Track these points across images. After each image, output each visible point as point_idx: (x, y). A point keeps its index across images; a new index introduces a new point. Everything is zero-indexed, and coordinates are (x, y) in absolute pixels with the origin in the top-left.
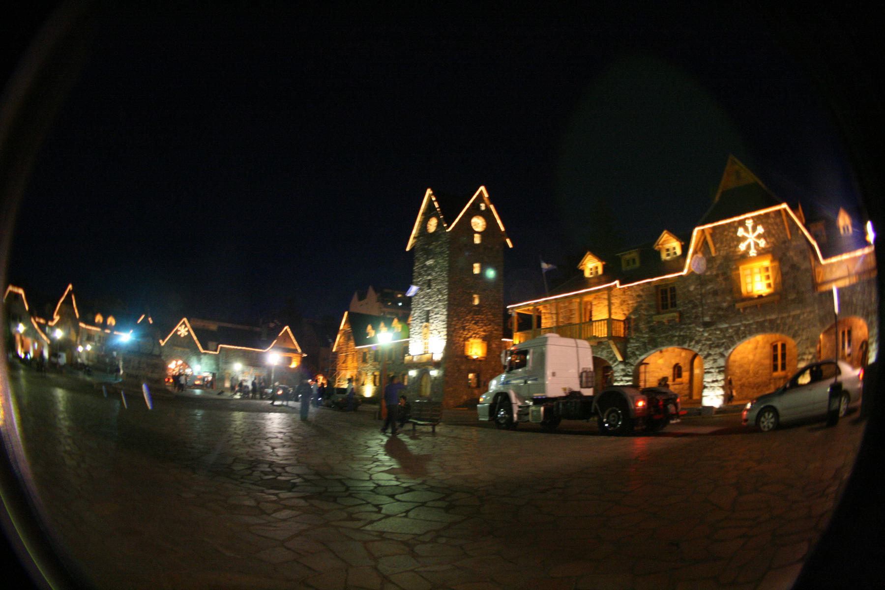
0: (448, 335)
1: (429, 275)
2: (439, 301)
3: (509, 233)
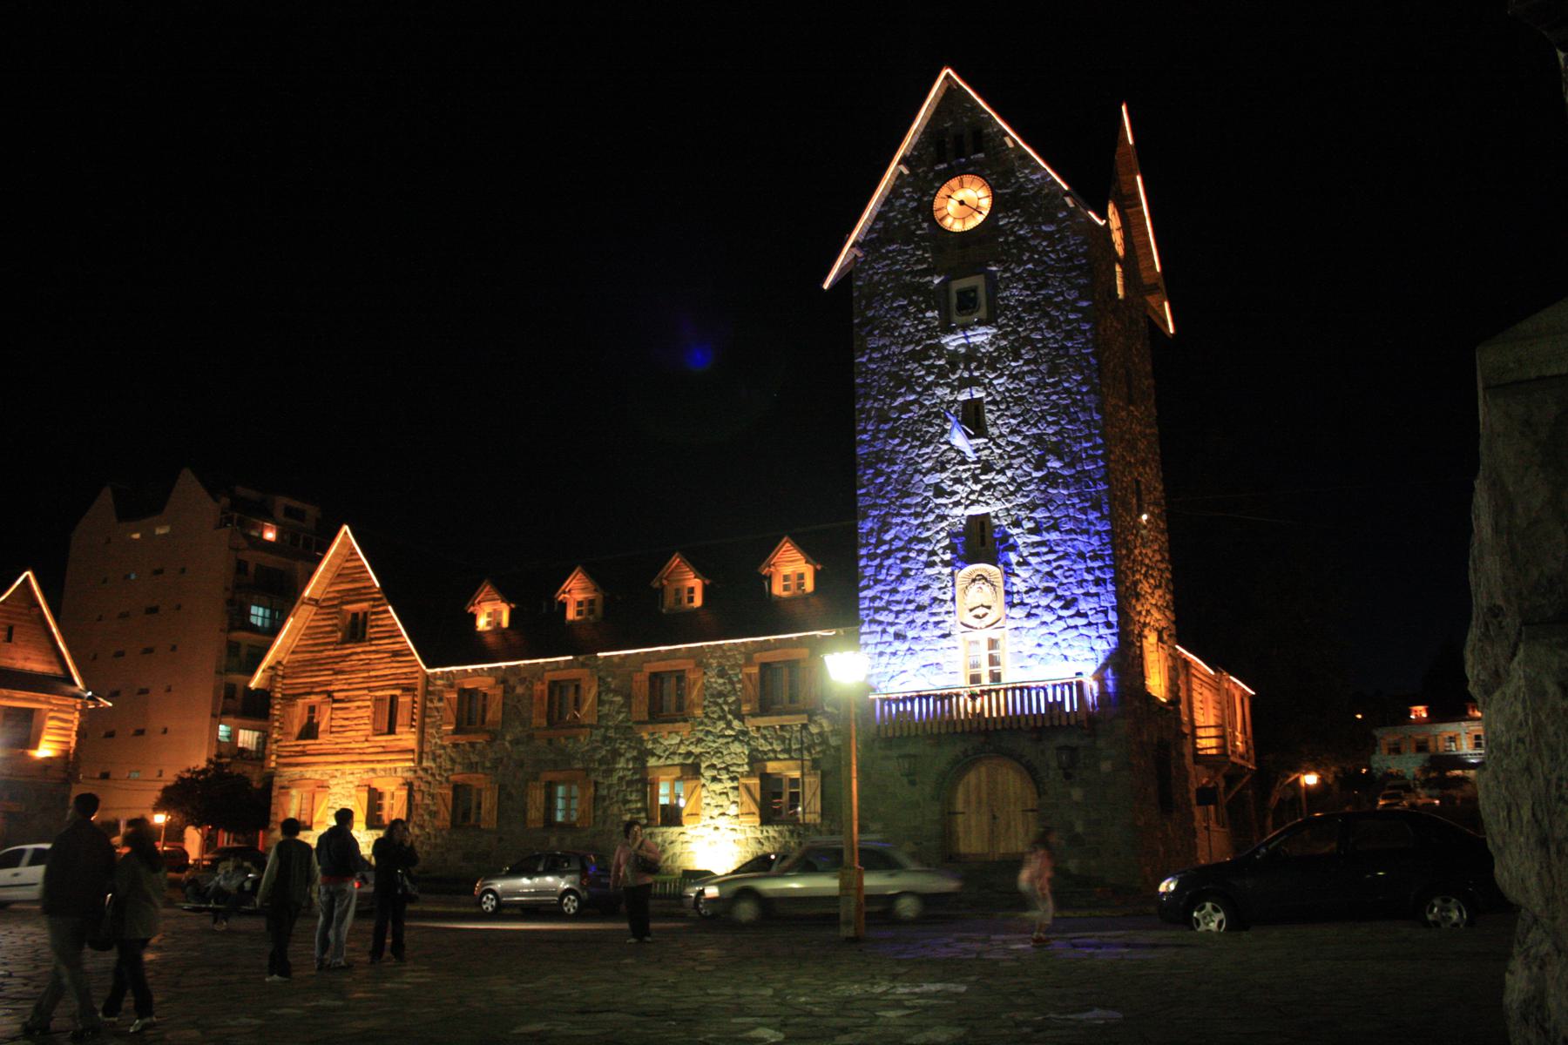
0: (1121, 610)
1: (972, 382)
2: (1051, 479)
3: (1173, 282)
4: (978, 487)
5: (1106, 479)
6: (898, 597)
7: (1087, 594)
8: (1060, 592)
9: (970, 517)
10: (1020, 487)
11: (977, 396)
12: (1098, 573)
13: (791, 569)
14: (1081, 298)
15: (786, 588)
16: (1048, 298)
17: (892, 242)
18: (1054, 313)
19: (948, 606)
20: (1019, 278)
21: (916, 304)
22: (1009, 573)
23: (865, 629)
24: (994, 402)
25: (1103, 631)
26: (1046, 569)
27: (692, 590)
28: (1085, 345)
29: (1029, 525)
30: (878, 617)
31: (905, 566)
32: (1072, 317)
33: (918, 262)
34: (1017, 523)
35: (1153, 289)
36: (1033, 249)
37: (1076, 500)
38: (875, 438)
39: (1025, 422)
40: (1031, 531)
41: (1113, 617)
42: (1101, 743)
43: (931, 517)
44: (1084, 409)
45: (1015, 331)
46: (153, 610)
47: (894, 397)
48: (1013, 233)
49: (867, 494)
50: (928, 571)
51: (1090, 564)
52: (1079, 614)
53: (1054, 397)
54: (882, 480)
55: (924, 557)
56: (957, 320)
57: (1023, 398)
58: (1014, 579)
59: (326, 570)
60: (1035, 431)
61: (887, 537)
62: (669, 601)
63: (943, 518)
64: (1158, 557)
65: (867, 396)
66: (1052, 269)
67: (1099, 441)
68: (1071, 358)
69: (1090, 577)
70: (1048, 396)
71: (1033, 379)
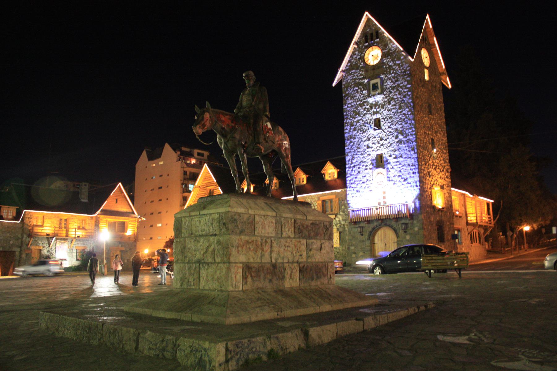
0: (420, 181)
2: (400, 142)
3: (450, 71)
4: (379, 145)
5: (416, 141)
6: (357, 179)
7: (410, 177)
8: (403, 176)
9: (377, 155)
10: (391, 145)
11: (378, 117)
12: (414, 170)
13: (330, 172)
14: (408, 84)
15: (330, 177)
16: (398, 85)
17: (353, 69)
18: (400, 89)
19: (371, 182)
20: (390, 79)
21: (361, 89)
22: (388, 171)
23: (348, 189)
24: (383, 119)
25: (416, 188)
26: (399, 169)
27: (303, 179)
28: (409, 99)
29: (394, 156)
30: (352, 186)
31: (359, 170)
32: (405, 90)
33: (360, 75)
34: (390, 156)
35: (443, 74)
36: (394, 69)
37: (407, 148)
38: (350, 131)
39: (392, 124)
40: (394, 158)
41: (418, 184)
42: (415, 222)
43: (366, 155)
44: (409, 119)
45: (389, 96)
46: (160, 188)
47: (355, 118)
48: (388, 64)
49: (348, 148)
50: (366, 171)
51: (412, 168)
52: (408, 183)
53: (401, 116)
54: (352, 144)
55: (364, 167)
56: (372, 93)
57: (391, 117)
58: (389, 173)
59: (201, 177)
60: (395, 127)
61: (354, 161)
62: (297, 182)
63: (370, 155)
64: (443, 162)
65: (347, 118)
66: (399, 75)
67: (414, 129)
68: (405, 104)
69: (411, 172)
70: (399, 116)
71: (394, 111)
